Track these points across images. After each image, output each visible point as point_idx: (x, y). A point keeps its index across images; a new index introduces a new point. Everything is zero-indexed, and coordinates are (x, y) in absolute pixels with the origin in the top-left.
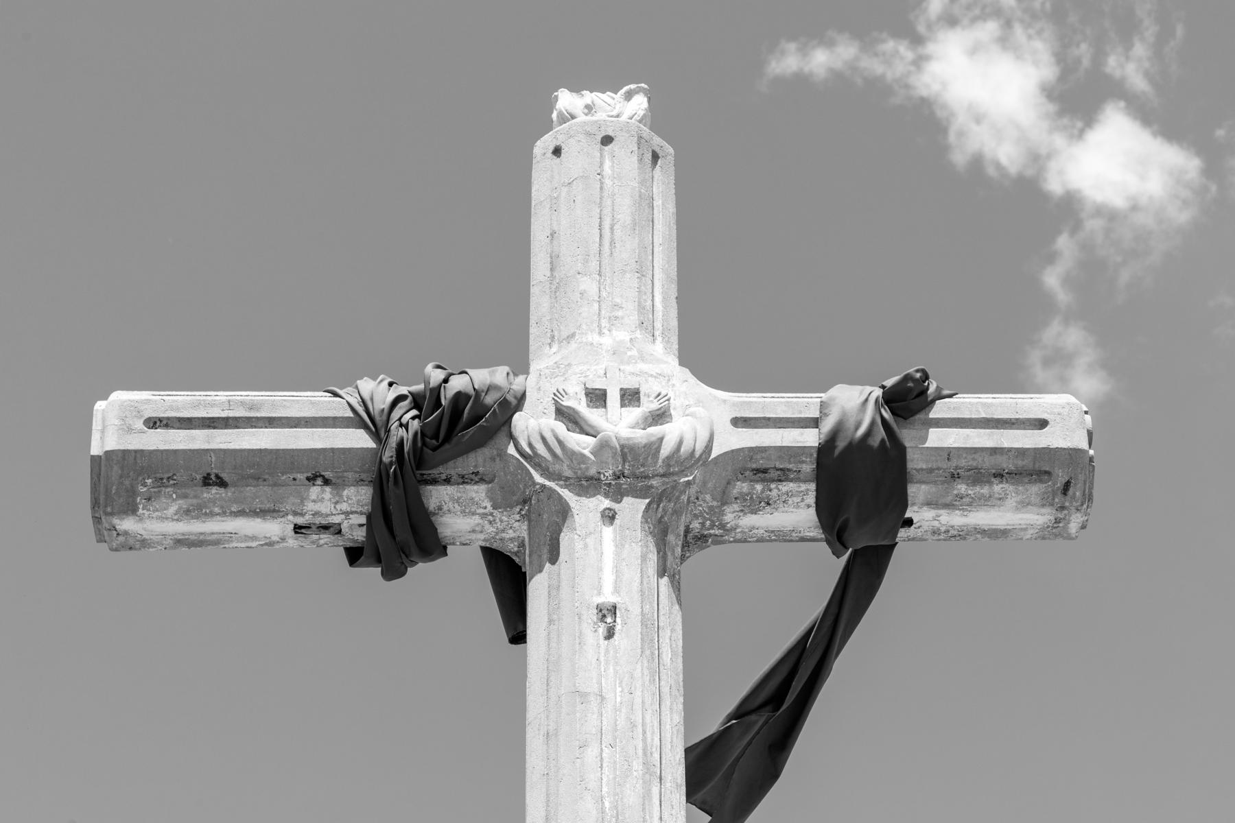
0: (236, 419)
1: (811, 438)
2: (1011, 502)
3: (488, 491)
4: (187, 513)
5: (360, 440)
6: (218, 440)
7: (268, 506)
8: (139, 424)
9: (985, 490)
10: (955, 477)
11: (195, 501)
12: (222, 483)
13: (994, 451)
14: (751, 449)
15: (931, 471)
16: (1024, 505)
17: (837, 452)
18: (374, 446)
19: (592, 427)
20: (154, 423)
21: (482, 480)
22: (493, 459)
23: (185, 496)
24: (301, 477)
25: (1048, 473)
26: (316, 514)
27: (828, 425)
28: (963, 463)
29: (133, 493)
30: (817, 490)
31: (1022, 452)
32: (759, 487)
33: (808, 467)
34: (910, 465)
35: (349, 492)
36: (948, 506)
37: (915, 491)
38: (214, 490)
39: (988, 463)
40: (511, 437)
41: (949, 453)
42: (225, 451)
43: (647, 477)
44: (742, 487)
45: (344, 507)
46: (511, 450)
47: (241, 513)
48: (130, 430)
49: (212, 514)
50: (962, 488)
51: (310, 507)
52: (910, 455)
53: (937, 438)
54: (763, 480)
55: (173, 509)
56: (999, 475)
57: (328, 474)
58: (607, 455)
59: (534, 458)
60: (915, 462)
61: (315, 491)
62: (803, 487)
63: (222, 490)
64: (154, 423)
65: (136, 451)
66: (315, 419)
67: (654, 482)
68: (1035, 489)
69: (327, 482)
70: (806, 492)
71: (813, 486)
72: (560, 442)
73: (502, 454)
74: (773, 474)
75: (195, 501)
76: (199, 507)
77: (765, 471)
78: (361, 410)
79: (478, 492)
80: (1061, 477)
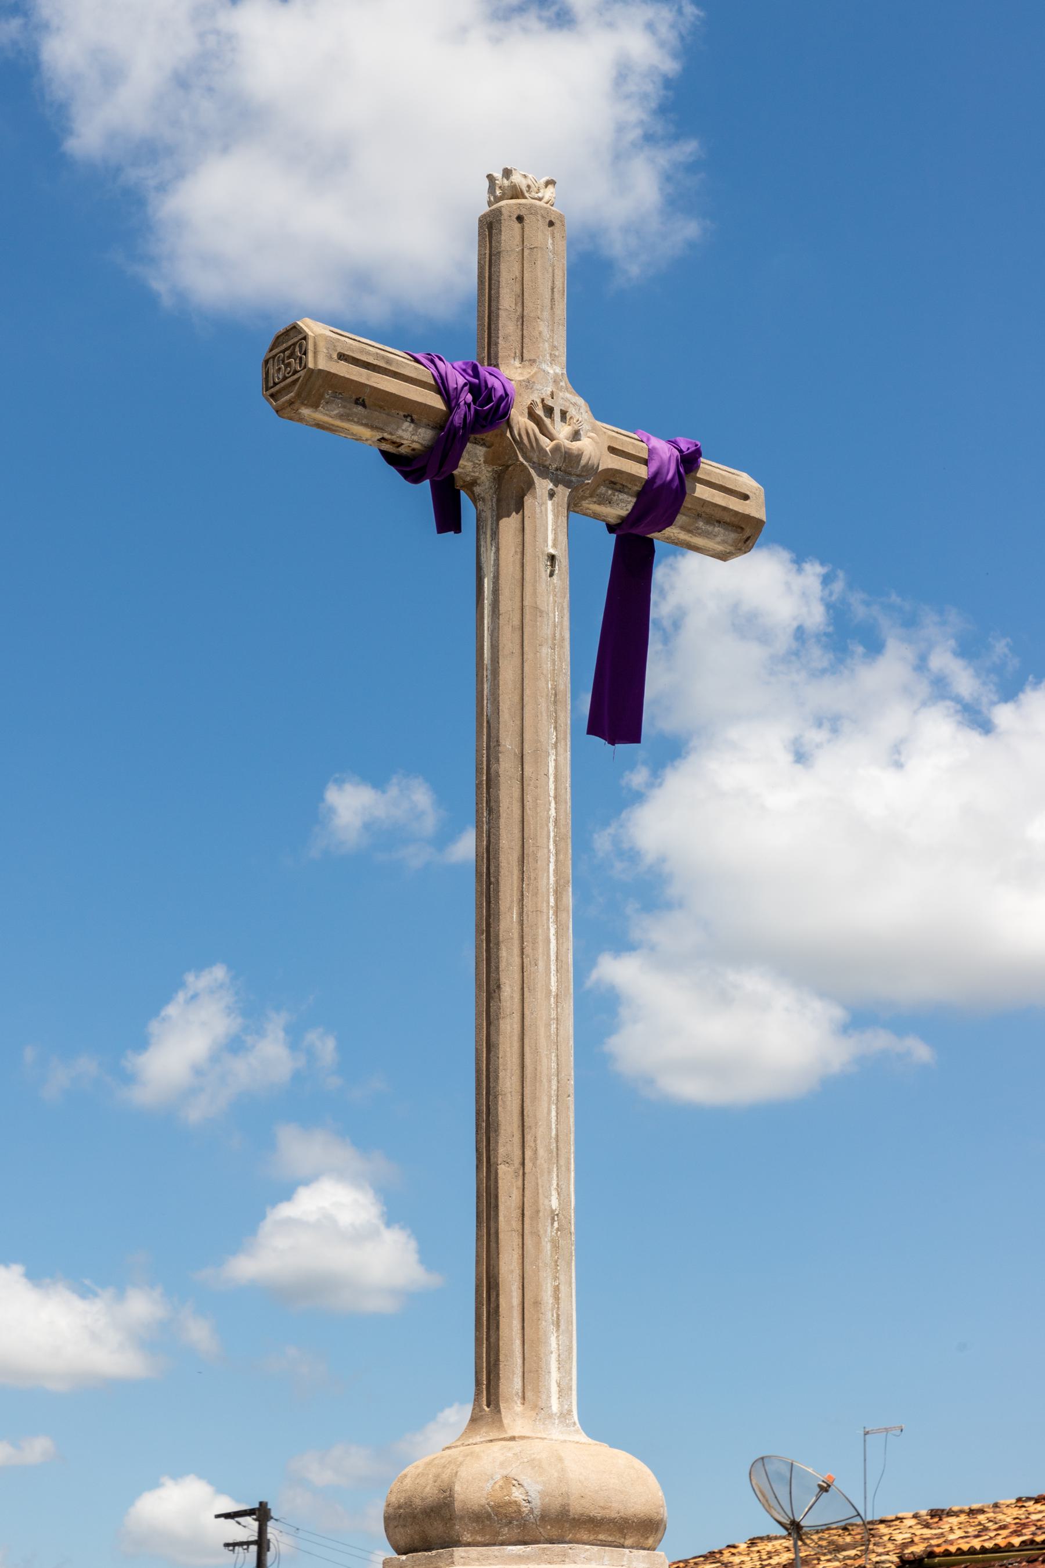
0: (380, 367)
1: (642, 472)
2: (718, 539)
3: (486, 452)
4: (341, 417)
5: (436, 402)
6: (373, 380)
7: (381, 425)
8: (335, 356)
9: (710, 528)
10: (699, 516)
11: (348, 411)
12: (364, 405)
13: (725, 509)
14: (616, 470)
15: (690, 509)
16: (724, 542)
17: (655, 486)
18: (443, 407)
19: (551, 434)
20: (342, 357)
21: (484, 445)
22: (497, 435)
23: (344, 407)
24: (402, 413)
25: (742, 529)
26: (401, 437)
27: (654, 466)
28: (708, 510)
29: (322, 396)
30: (636, 503)
31: (736, 513)
32: (610, 492)
33: (637, 488)
34: (684, 504)
35: (421, 430)
36: (689, 531)
37: (680, 519)
38: (360, 408)
39: (719, 514)
40: (509, 425)
41: (704, 503)
42: (375, 388)
43: (570, 474)
44: (603, 489)
45: (415, 438)
46: (508, 434)
47: (366, 425)
48: (330, 358)
49: (352, 421)
50: (701, 524)
51: (400, 432)
52: (687, 498)
53: (702, 492)
54: (612, 489)
55: (336, 412)
56: (719, 522)
57: (415, 417)
58: (558, 456)
59: (520, 443)
60: (687, 503)
61: (407, 424)
62: (630, 499)
63: (363, 409)
64: (342, 357)
65: (334, 374)
66: (416, 380)
67: (573, 479)
68: (733, 536)
69: (412, 421)
70: (629, 503)
71: (634, 500)
72: (536, 439)
73: (503, 434)
74: (618, 487)
75: (348, 411)
76: (348, 415)
77: (615, 483)
78: (439, 381)
79: (480, 451)
80: (748, 532)
